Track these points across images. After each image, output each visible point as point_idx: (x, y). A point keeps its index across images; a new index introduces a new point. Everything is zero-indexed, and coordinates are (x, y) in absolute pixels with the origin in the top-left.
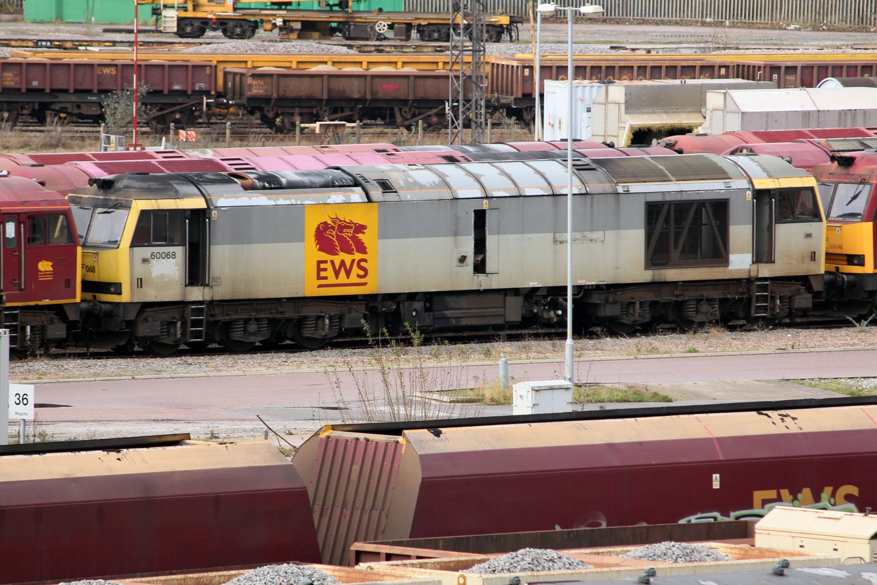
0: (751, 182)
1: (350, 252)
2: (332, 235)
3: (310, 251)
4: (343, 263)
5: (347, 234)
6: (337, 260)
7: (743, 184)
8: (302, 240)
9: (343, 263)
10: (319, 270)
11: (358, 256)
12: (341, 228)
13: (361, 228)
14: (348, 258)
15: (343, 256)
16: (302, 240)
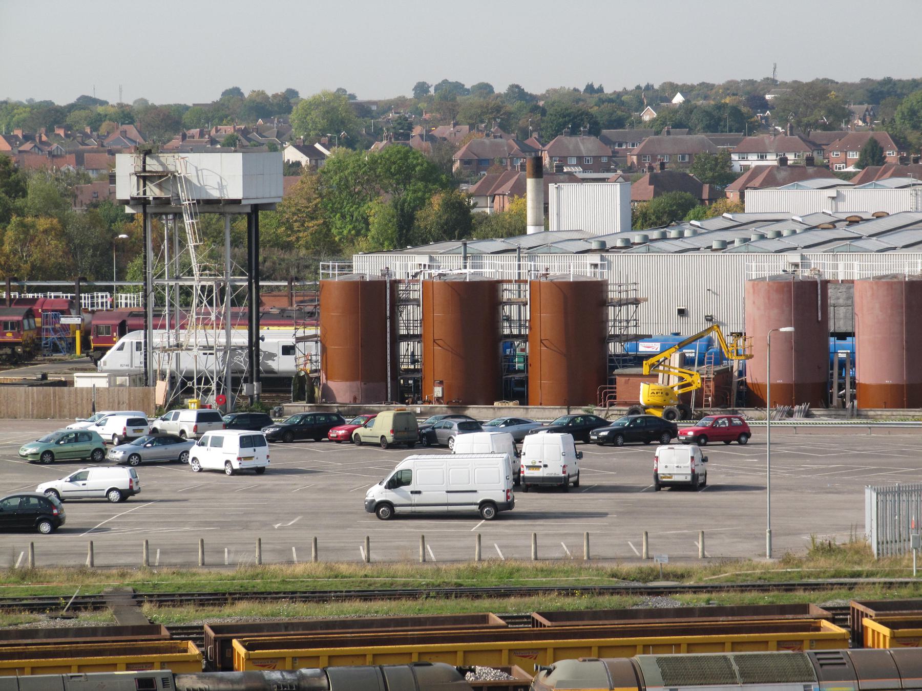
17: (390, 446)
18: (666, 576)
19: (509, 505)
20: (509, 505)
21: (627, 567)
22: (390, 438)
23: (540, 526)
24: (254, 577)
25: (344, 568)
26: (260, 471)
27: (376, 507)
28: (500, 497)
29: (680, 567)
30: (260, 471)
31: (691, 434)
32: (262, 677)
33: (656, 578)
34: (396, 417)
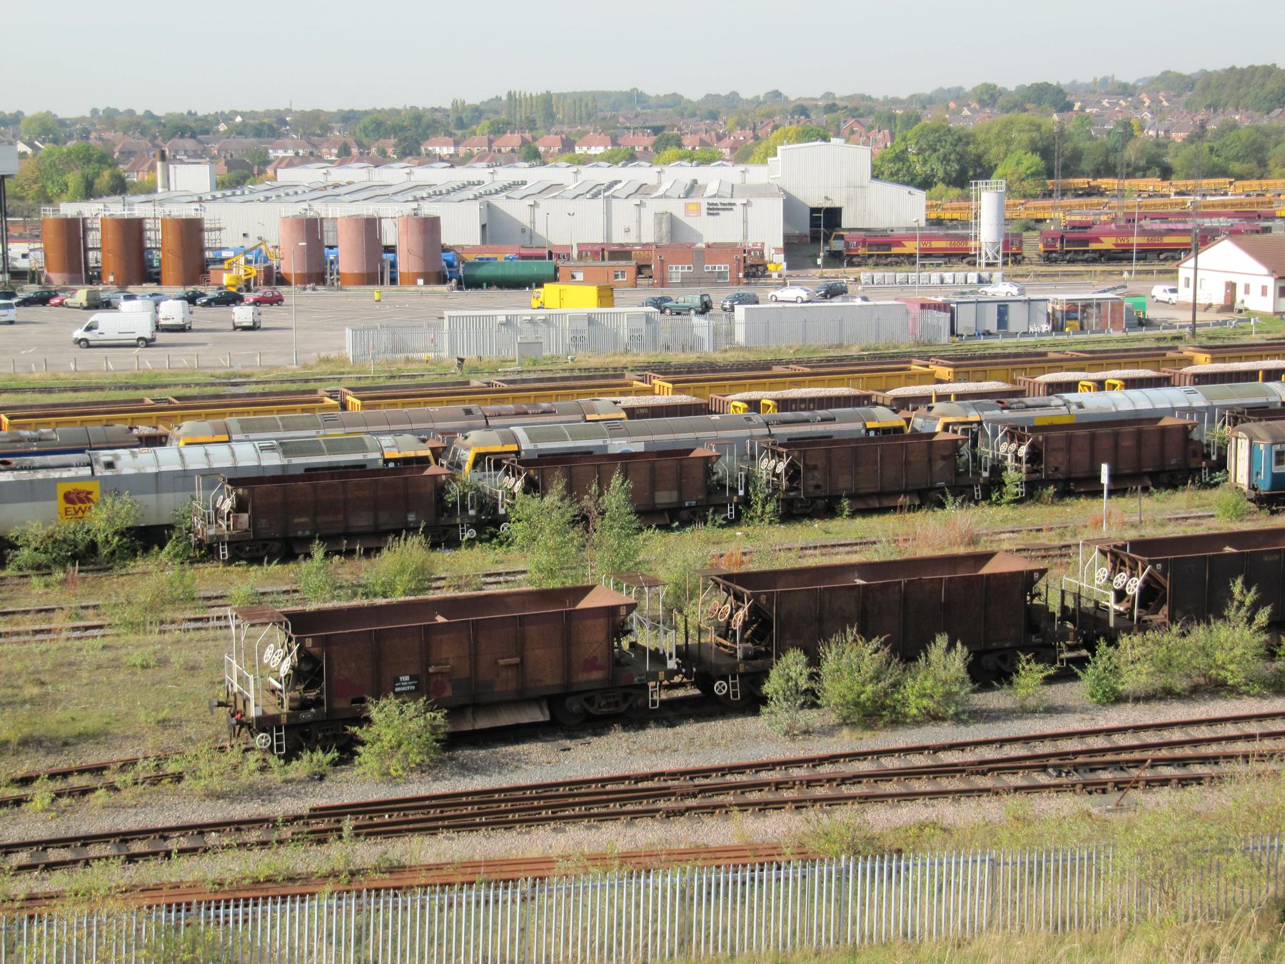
0: (383, 454)
1: (83, 502)
2: (73, 496)
3: (61, 504)
4: (80, 508)
5: (82, 496)
6: (77, 507)
7: (377, 455)
8: (55, 498)
9: (80, 508)
10: (66, 511)
11: (88, 505)
12: (78, 493)
13: (90, 493)
14: (83, 506)
15: (80, 505)
16: (55, 498)
17: (85, 308)
18: (241, 376)
19: (153, 340)
20: (153, 340)
21: (219, 372)
22: (85, 304)
23: (170, 350)
24: (10, 380)
25: (62, 375)
26: (11, 323)
27: (78, 342)
28: (148, 336)
29: (248, 371)
30: (11, 323)
31: (252, 300)
32: (19, 434)
33: (235, 377)
34: (88, 292)
